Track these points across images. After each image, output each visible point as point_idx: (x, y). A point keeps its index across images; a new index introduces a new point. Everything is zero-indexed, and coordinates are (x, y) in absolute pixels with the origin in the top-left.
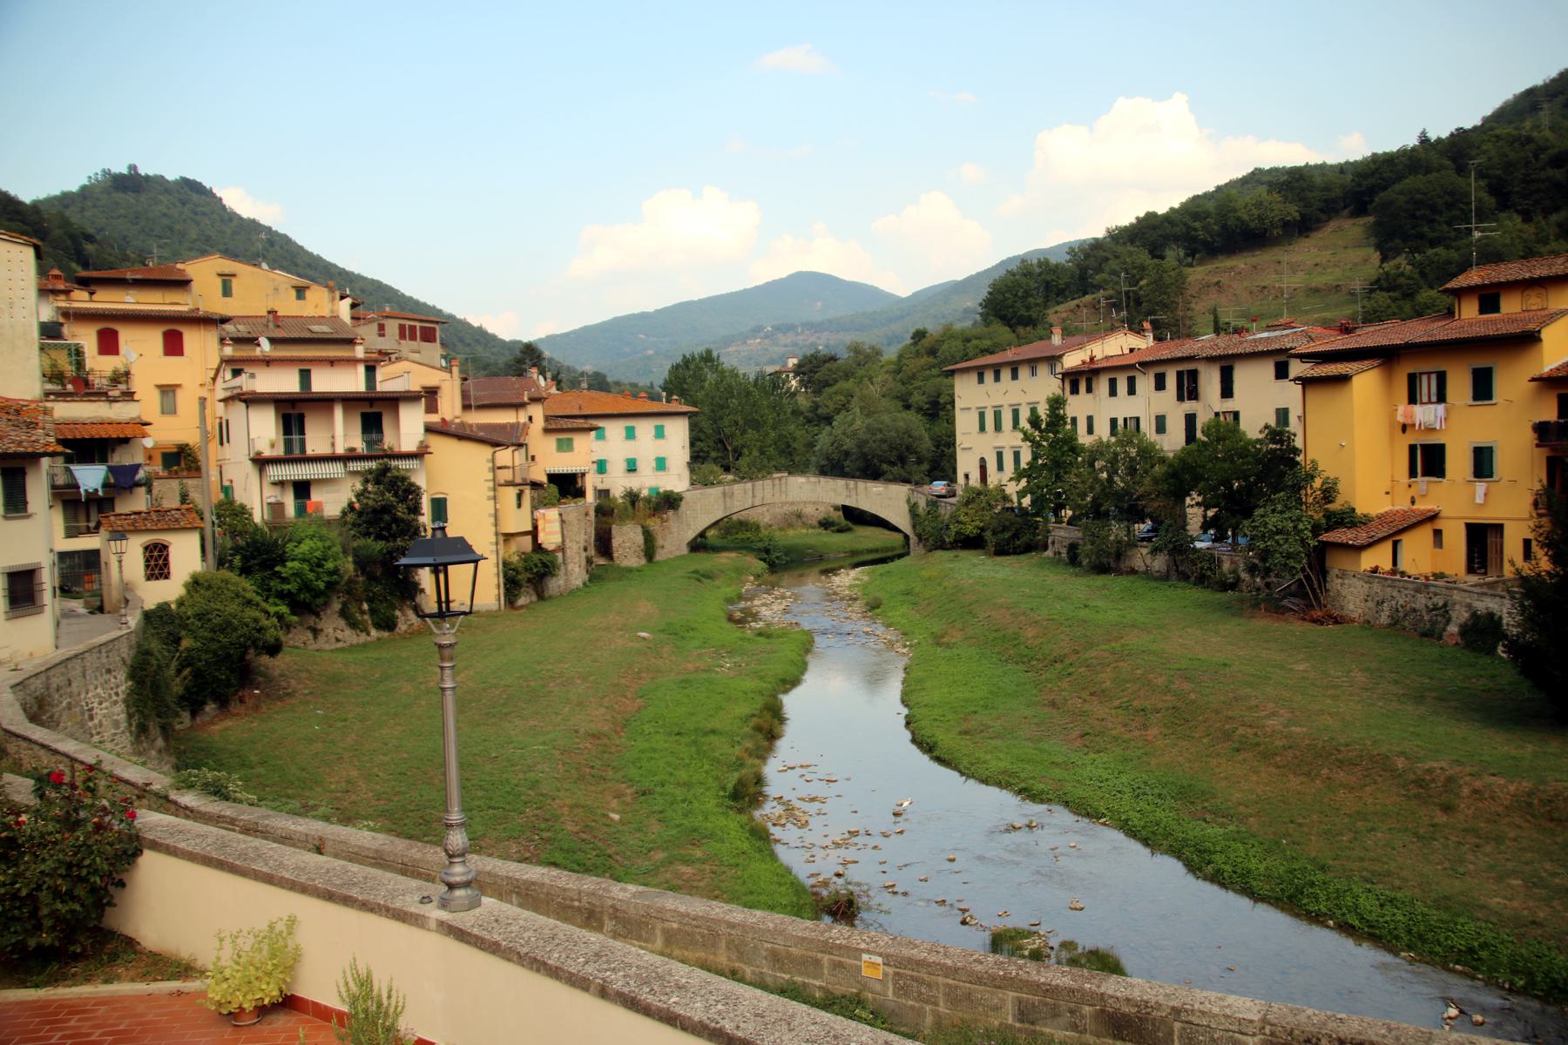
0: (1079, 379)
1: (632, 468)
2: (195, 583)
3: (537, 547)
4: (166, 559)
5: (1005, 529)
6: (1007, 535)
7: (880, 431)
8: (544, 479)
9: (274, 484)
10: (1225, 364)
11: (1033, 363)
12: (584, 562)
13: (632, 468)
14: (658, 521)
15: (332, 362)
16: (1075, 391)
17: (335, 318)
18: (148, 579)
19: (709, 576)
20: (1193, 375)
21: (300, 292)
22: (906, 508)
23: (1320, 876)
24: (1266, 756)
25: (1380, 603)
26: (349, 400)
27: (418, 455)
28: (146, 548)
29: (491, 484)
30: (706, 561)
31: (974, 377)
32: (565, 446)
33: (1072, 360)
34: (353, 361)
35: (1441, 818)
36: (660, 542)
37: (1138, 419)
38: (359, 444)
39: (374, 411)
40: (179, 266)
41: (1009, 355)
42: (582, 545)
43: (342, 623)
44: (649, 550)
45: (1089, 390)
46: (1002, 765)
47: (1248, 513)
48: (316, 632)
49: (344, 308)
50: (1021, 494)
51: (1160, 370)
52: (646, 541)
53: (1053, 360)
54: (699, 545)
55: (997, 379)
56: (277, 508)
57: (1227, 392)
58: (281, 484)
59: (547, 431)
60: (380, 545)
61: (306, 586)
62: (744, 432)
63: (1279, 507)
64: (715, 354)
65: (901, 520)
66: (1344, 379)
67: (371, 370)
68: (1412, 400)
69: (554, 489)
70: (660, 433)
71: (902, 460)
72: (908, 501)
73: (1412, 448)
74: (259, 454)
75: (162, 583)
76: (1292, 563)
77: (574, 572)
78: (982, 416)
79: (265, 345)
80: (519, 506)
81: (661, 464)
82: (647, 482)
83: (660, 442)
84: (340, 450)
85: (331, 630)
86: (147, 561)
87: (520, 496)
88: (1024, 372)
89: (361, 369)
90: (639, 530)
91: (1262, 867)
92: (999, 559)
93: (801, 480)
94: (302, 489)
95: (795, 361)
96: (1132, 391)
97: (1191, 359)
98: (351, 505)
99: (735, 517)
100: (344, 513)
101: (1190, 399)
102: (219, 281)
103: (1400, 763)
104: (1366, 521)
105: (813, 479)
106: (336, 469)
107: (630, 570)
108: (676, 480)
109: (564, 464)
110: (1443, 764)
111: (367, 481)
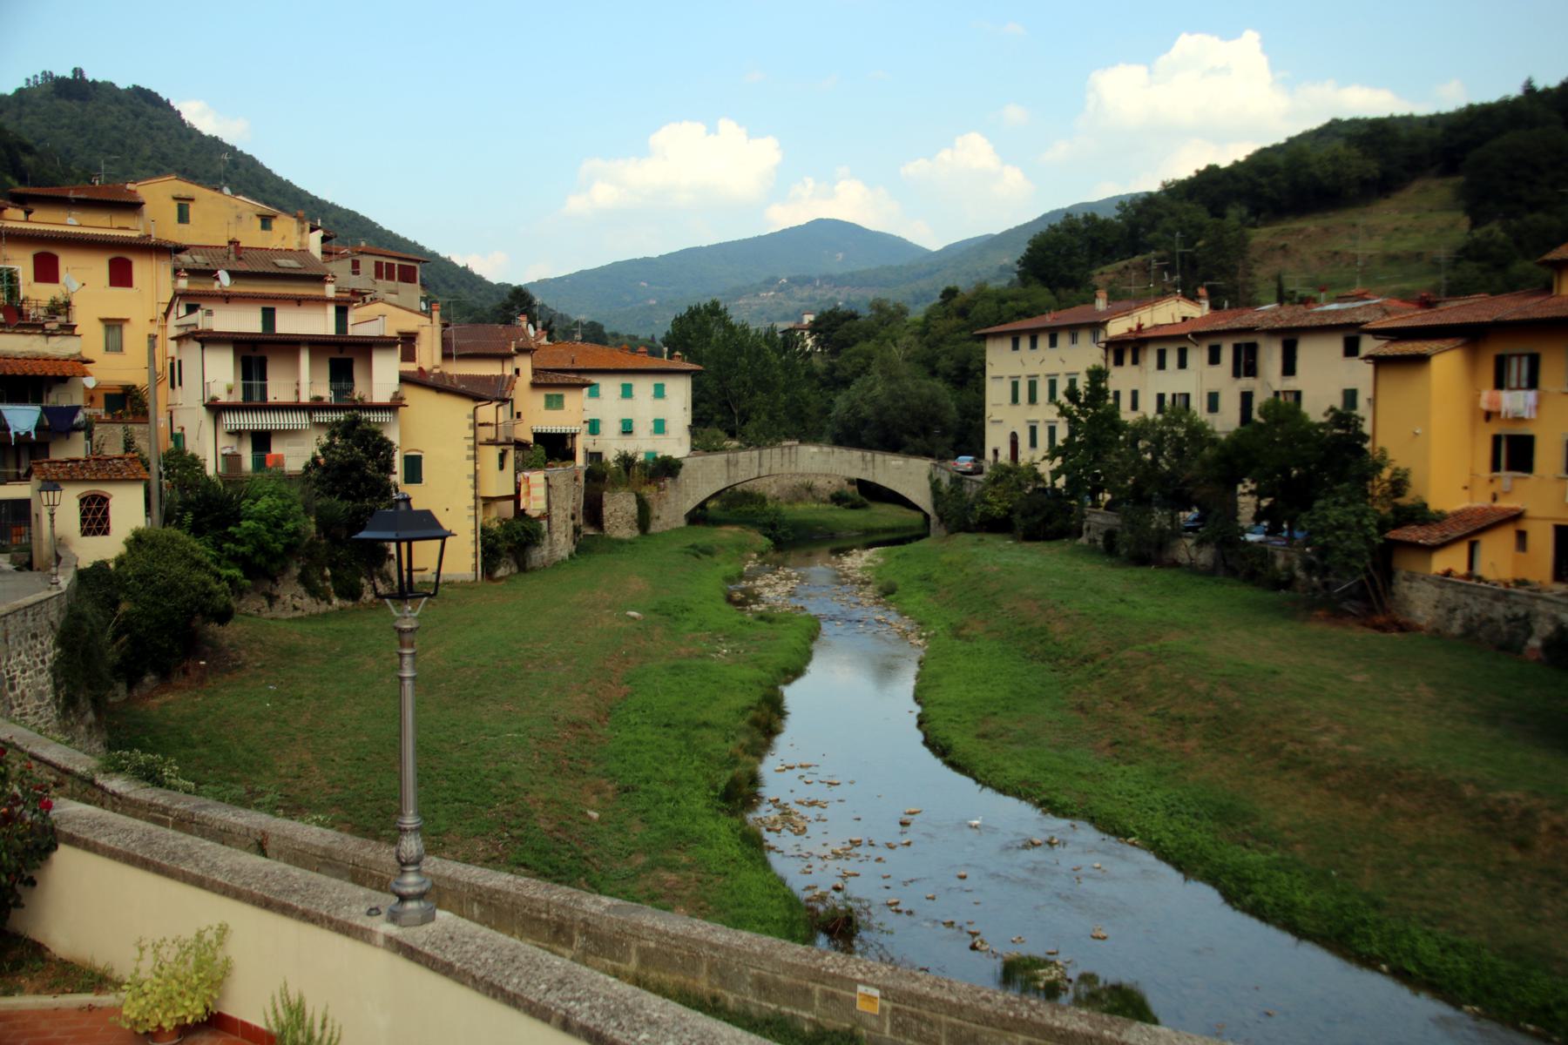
0: (1126, 349)
1: (627, 429)
2: (137, 541)
3: (520, 513)
4: (106, 513)
5: (1035, 512)
6: (1037, 519)
7: (903, 398)
8: (531, 439)
9: (230, 433)
10: (1288, 337)
11: (1074, 330)
12: (571, 531)
13: (627, 429)
14: (655, 489)
15: (299, 301)
16: (1119, 362)
17: (304, 252)
18: (85, 533)
19: (708, 551)
20: (1252, 349)
21: (266, 221)
22: (927, 485)
23: (1372, 915)
24: (1318, 775)
25: (1452, 610)
26: (316, 345)
27: (394, 406)
28: (83, 501)
29: (471, 442)
30: (705, 536)
31: (1008, 343)
32: (554, 403)
33: (1118, 327)
34: (323, 301)
35: (1514, 856)
36: (656, 512)
37: (1187, 396)
38: (325, 392)
39: (344, 356)
40: (130, 186)
41: (1048, 320)
42: (569, 512)
43: (301, 590)
44: (644, 519)
45: (1135, 362)
46: (1024, 773)
47: (1307, 506)
48: (272, 599)
49: (314, 241)
50: (1055, 474)
51: (1214, 342)
52: (640, 510)
53: (1096, 327)
54: (698, 517)
55: (1034, 345)
56: (232, 460)
57: (1289, 369)
58: (237, 434)
59: (535, 386)
60: (347, 504)
61: (262, 548)
62: (752, 394)
63: (1342, 499)
64: (722, 307)
65: (920, 494)
66: (1422, 360)
67: (342, 312)
68: (1500, 384)
69: (541, 450)
70: (659, 393)
71: (926, 431)
72: (930, 477)
73: (1497, 440)
74: (214, 399)
75: (100, 539)
76: (1354, 562)
77: (560, 542)
78: (1015, 386)
79: (225, 279)
80: (502, 467)
81: (659, 426)
82: (643, 445)
83: (660, 402)
84: (305, 399)
85: (288, 597)
86: (84, 514)
87: (502, 457)
88: (1063, 340)
89: (331, 310)
90: (633, 498)
91: (1308, 902)
92: (1027, 545)
93: (813, 449)
94: (261, 440)
95: (811, 318)
96: (1182, 364)
97: (1249, 330)
98: (315, 459)
99: (739, 488)
100: (307, 468)
101: (1247, 375)
102: (174, 205)
103: (1469, 791)
104: (1440, 518)
105: (826, 449)
106: (299, 420)
107: (621, 542)
108: (676, 445)
109: (553, 422)
110: (1518, 794)
111: (332, 435)
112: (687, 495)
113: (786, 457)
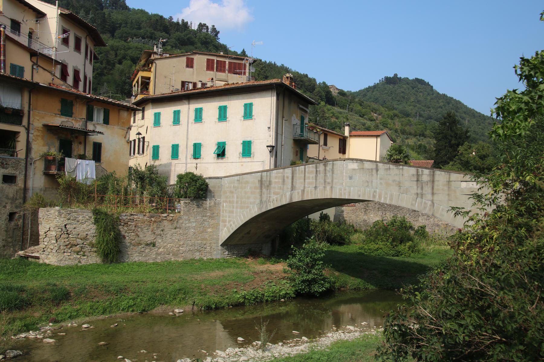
1: (221, 154)
70: (248, 113)
81: (247, 149)
83: (249, 122)
112: (224, 221)
113: (321, 175)
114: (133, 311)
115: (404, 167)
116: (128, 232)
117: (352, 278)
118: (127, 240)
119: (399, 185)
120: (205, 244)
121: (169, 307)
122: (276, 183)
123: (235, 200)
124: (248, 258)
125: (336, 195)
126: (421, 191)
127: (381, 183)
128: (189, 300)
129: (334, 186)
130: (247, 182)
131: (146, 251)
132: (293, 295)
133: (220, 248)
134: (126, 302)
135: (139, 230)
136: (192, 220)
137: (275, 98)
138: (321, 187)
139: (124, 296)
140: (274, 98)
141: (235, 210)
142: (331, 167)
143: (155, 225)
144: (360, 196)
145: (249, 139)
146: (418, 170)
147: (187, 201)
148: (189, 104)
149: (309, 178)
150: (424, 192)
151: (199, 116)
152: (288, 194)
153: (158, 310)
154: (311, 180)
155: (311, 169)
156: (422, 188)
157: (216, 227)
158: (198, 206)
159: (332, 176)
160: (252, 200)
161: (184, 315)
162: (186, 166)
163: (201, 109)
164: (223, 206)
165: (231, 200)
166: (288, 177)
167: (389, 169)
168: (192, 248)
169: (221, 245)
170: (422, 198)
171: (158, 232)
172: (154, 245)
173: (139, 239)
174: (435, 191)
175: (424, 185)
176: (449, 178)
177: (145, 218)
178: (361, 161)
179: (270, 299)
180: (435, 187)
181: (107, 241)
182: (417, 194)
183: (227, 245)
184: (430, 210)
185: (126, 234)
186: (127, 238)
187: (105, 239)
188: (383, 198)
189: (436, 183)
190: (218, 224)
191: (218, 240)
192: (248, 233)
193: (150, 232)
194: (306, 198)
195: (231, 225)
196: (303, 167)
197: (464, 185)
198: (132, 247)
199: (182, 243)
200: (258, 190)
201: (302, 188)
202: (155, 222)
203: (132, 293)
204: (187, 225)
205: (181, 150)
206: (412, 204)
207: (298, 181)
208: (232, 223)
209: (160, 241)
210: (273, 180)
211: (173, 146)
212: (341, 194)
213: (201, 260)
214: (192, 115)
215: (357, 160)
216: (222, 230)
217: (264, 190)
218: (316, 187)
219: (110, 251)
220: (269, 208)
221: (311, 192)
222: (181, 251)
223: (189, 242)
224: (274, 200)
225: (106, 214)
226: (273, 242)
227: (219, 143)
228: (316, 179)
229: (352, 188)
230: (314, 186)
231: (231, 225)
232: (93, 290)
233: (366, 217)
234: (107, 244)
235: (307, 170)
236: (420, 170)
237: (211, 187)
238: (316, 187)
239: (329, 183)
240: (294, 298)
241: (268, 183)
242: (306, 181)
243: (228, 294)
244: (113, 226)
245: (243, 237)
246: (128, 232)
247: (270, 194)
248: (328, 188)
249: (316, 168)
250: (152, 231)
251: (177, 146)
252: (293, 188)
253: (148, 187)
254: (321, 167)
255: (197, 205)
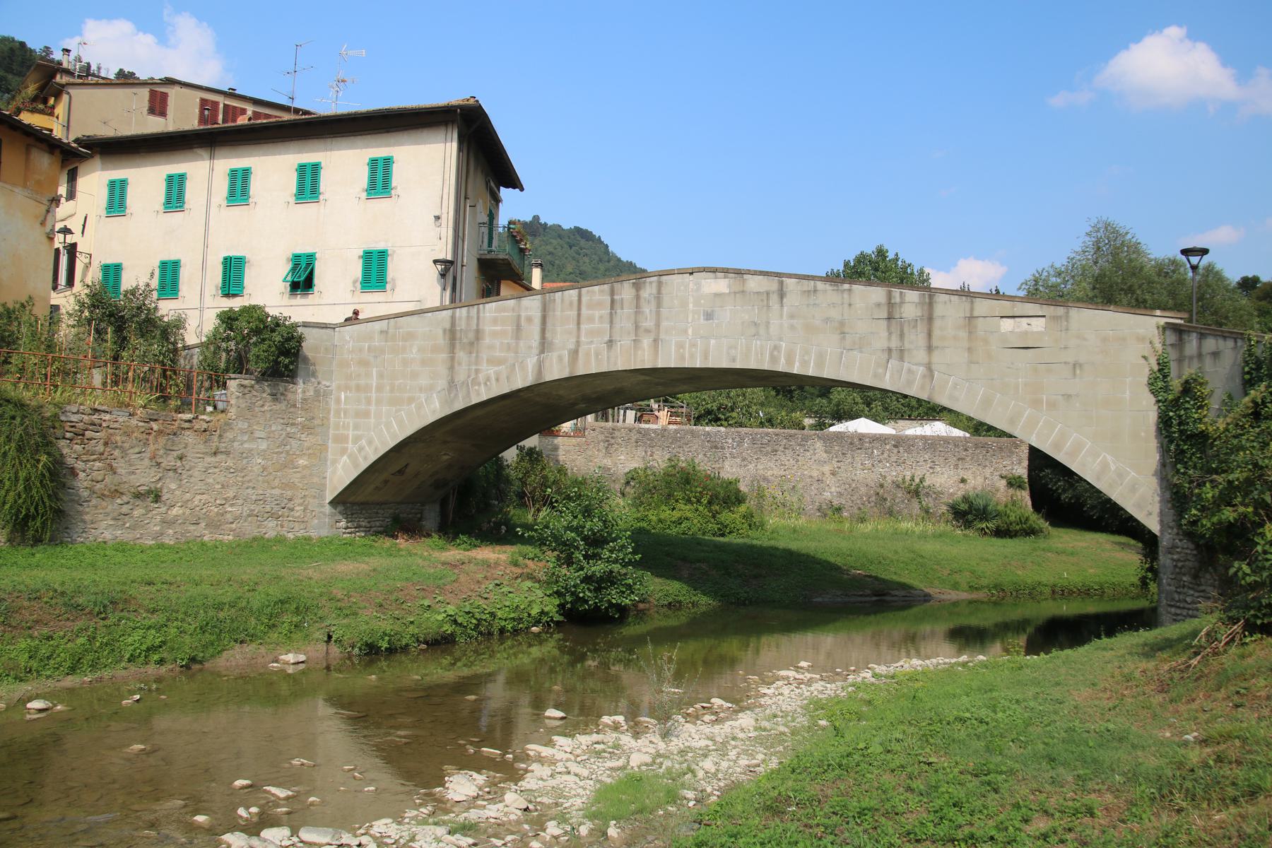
1: (302, 282)
13: (302, 282)
22: (1147, 411)
70: (380, 180)
81: (375, 269)
83: (381, 205)
112: (341, 439)
114: (161, 662)
115: (854, 287)
116: (85, 458)
117: (657, 580)
118: (82, 482)
119: (841, 329)
120: (290, 500)
121: (263, 650)
122: (494, 334)
123: (374, 382)
124: (395, 537)
125: (669, 359)
126: (899, 344)
127: (792, 327)
128: (312, 629)
129: (662, 336)
130: (410, 336)
131: (136, 513)
132: (557, 618)
133: (328, 509)
134: (137, 636)
135: (117, 453)
136: (257, 434)
137: (455, 145)
138: (624, 342)
139: (128, 619)
140: (454, 145)
141: (373, 408)
142: (654, 291)
143: (162, 440)
144: (734, 360)
145: (380, 246)
146: (890, 292)
147: (246, 382)
148: (212, 157)
149: (591, 319)
150: (907, 346)
151: (239, 187)
152: (531, 362)
153: (234, 658)
154: (597, 325)
155: (597, 297)
156: (902, 336)
157: (319, 454)
158: (275, 396)
159: (658, 313)
160: (424, 382)
161: (307, 668)
162: (201, 316)
163: (246, 173)
164: (338, 401)
165: (362, 382)
166: (529, 319)
167: (815, 291)
168: (257, 509)
169: (331, 503)
170: (902, 359)
171: (169, 461)
172: (157, 498)
173: (117, 479)
174: (935, 342)
175: (906, 330)
176: (972, 309)
177: (134, 422)
178: (739, 272)
179: (509, 627)
180: (936, 333)
181: (27, 479)
182: (890, 350)
183: (344, 503)
184: (923, 387)
185: (79, 465)
186: (82, 475)
187: (22, 475)
188: (797, 364)
189: (937, 324)
190: (323, 448)
191: (322, 488)
192: (401, 472)
193: (147, 462)
194: (581, 370)
195: (361, 449)
196: (574, 293)
197: (1007, 325)
198: (94, 502)
199: (231, 494)
200: (444, 356)
201: (572, 346)
202: (160, 432)
203: (148, 611)
204: (246, 446)
205: (184, 274)
206: (875, 375)
207: (559, 329)
208: (364, 442)
209: (173, 486)
210: (487, 328)
211: (164, 265)
212: (682, 358)
213: (280, 540)
214: (222, 186)
215: (726, 271)
216: (334, 462)
217: (461, 355)
218: (610, 343)
219: (36, 509)
220: (475, 400)
221: (597, 355)
222: (228, 516)
223: (250, 491)
224: (488, 379)
225: (20, 405)
226: (444, 503)
227: (297, 257)
228: (611, 322)
229: (713, 342)
230: (607, 338)
231: (361, 449)
232: (26, 603)
233: (608, 462)
234: (28, 488)
235: (584, 299)
236: (896, 292)
237: (307, 348)
238: (610, 343)
239: (648, 331)
240: (558, 623)
241: (471, 335)
242: (583, 327)
243: (410, 613)
244: (44, 436)
245: (386, 482)
246: (85, 458)
247: (477, 364)
248: (646, 342)
249: (612, 293)
250: (153, 458)
251: (176, 265)
252: (544, 345)
253: (134, 340)
254: (626, 291)
255: (272, 395)
